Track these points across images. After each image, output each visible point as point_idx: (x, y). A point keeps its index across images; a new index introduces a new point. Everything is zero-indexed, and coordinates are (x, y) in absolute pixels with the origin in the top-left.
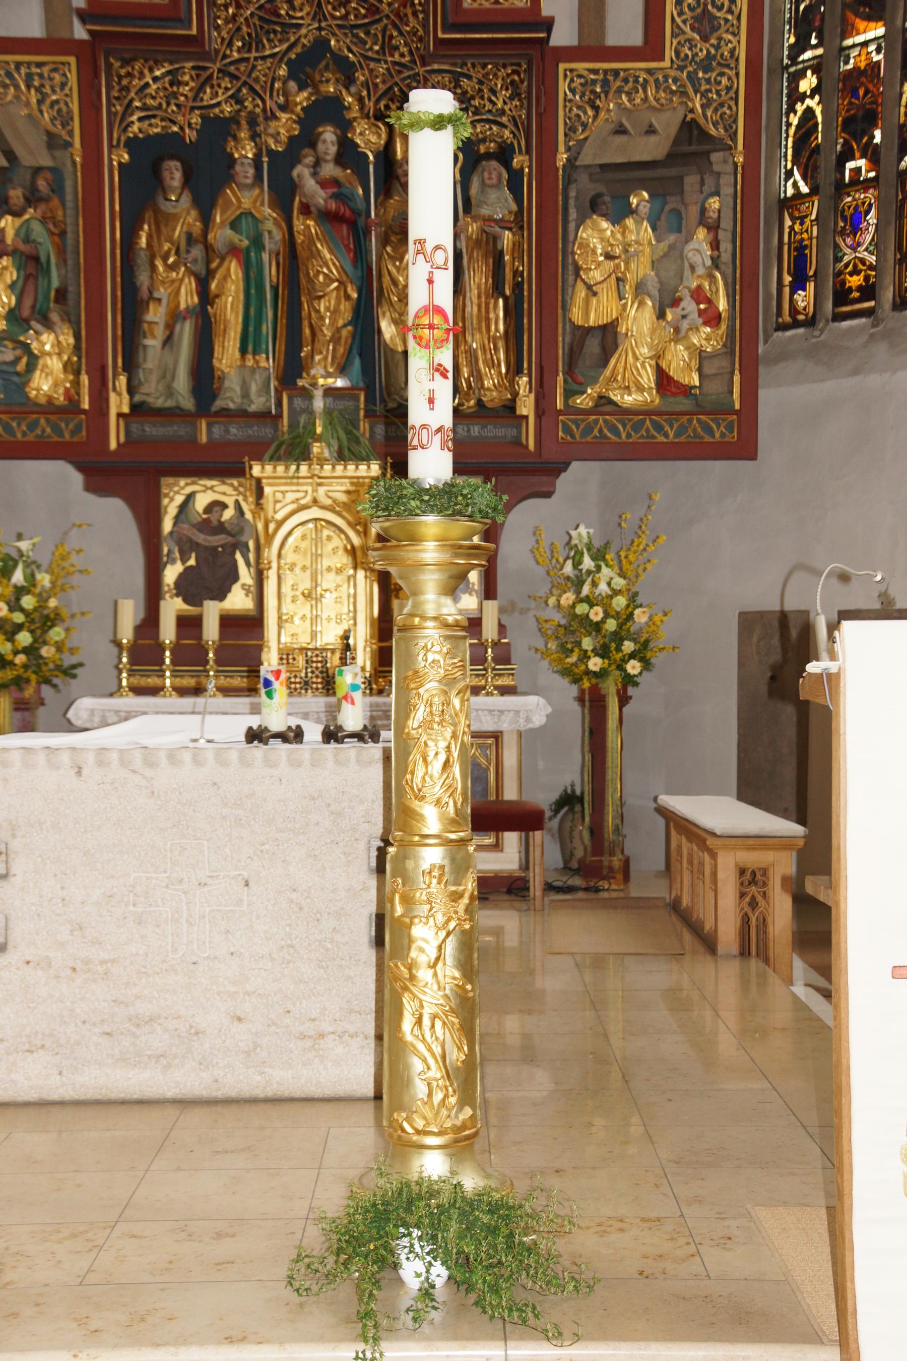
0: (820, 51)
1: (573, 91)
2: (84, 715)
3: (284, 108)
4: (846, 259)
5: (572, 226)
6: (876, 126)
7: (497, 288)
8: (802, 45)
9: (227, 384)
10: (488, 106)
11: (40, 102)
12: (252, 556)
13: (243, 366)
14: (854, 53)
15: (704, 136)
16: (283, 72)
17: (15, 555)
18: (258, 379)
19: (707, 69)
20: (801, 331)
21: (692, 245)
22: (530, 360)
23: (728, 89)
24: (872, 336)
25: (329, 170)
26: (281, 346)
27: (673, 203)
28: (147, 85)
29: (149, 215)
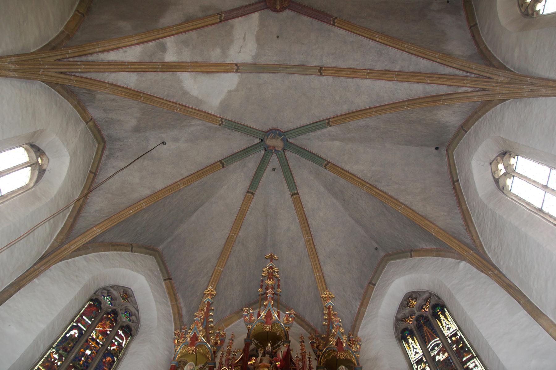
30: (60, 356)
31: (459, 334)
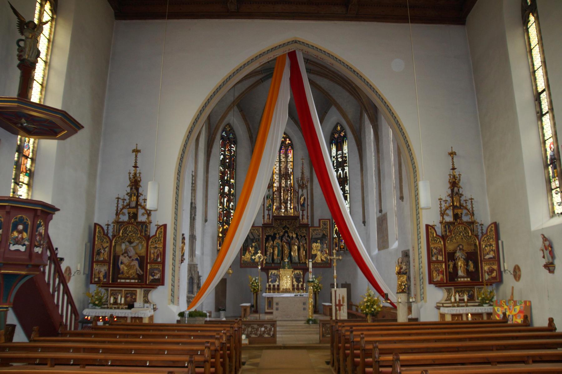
3: (282, 232)
7: (304, 250)
25: (287, 238)
30: (222, 167)
31: (347, 154)
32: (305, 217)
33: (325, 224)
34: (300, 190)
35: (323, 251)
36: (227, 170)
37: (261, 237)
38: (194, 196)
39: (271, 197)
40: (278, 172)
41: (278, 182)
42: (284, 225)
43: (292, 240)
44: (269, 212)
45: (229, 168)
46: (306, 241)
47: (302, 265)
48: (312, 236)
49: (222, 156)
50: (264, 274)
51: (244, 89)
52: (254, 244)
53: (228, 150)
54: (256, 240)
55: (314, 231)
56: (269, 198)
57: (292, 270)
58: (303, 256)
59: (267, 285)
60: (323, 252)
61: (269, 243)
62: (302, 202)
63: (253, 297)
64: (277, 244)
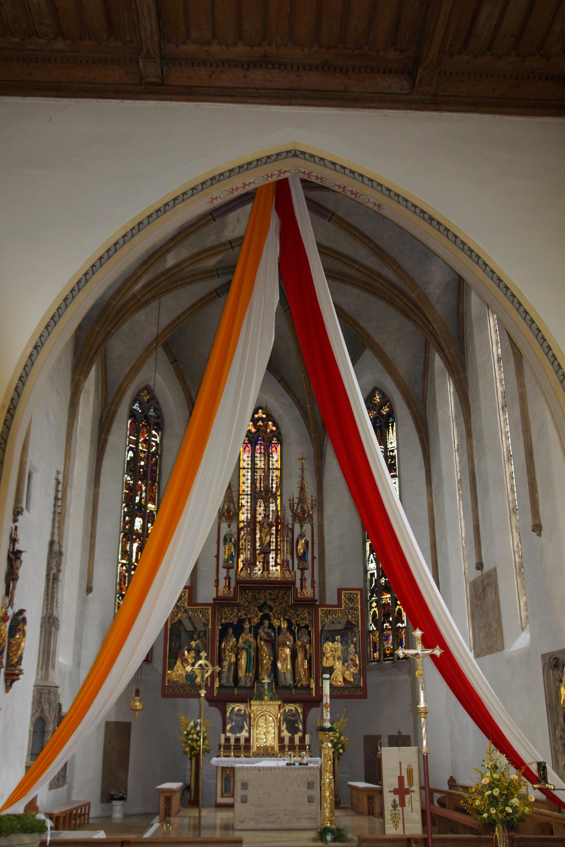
0: (376, 598)
1: (322, 614)
2: (214, 762)
3: (256, 616)
4: (386, 646)
5: (323, 644)
6: (390, 616)
7: (306, 658)
8: (372, 596)
9: (242, 680)
10: (303, 616)
11: (202, 616)
12: (248, 723)
13: (245, 676)
14: (384, 600)
15: (352, 624)
16: (257, 609)
17: (197, 723)
18: (249, 678)
19: (352, 610)
20: (376, 663)
21: (350, 648)
22: (314, 675)
23: (357, 614)
24: (393, 666)
25: (267, 630)
26: (254, 670)
27: (345, 638)
28: (226, 612)
29: (224, 639)
30: (131, 477)
31: (396, 451)
32: (308, 583)
33: (351, 600)
34: (297, 526)
35: (348, 659)
36: (140, 483)
37: (210, 627)
38: (59, 528)
39: (233, 540)
40: (249, 490)
41: (249, 512)
42: (262, 602)
43: (279, 634)
44: (228, 573)
45: (144, 478)
46: (310, 636)
47: (301, 691)
48: (323, 627)
49: (131, 452)
50: (215, 712)
51: (181, 311)
52: (193, 643)
53: (145, 441)
54: (199, 635)
55: (327, 614)
56: (228, 540)
57: (280, 702)
58: (301, 670)
59: (223, 737)
60: (347, 661)
61: (228, 641)
62: (302, 551)
63: (189, 766)
64: (244, 643)
